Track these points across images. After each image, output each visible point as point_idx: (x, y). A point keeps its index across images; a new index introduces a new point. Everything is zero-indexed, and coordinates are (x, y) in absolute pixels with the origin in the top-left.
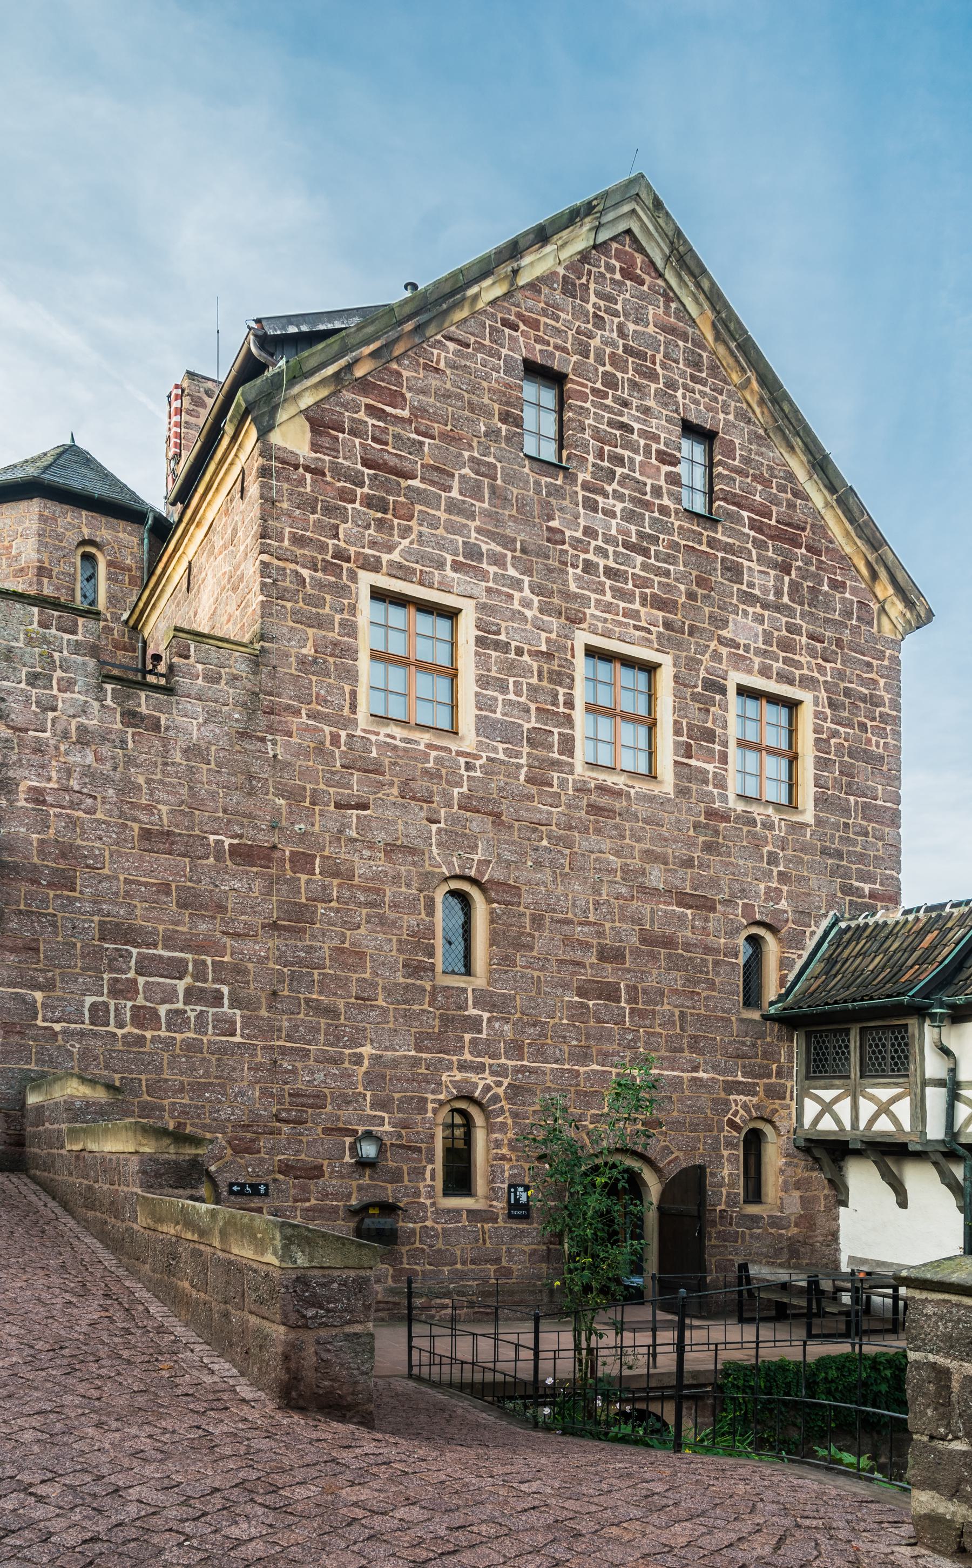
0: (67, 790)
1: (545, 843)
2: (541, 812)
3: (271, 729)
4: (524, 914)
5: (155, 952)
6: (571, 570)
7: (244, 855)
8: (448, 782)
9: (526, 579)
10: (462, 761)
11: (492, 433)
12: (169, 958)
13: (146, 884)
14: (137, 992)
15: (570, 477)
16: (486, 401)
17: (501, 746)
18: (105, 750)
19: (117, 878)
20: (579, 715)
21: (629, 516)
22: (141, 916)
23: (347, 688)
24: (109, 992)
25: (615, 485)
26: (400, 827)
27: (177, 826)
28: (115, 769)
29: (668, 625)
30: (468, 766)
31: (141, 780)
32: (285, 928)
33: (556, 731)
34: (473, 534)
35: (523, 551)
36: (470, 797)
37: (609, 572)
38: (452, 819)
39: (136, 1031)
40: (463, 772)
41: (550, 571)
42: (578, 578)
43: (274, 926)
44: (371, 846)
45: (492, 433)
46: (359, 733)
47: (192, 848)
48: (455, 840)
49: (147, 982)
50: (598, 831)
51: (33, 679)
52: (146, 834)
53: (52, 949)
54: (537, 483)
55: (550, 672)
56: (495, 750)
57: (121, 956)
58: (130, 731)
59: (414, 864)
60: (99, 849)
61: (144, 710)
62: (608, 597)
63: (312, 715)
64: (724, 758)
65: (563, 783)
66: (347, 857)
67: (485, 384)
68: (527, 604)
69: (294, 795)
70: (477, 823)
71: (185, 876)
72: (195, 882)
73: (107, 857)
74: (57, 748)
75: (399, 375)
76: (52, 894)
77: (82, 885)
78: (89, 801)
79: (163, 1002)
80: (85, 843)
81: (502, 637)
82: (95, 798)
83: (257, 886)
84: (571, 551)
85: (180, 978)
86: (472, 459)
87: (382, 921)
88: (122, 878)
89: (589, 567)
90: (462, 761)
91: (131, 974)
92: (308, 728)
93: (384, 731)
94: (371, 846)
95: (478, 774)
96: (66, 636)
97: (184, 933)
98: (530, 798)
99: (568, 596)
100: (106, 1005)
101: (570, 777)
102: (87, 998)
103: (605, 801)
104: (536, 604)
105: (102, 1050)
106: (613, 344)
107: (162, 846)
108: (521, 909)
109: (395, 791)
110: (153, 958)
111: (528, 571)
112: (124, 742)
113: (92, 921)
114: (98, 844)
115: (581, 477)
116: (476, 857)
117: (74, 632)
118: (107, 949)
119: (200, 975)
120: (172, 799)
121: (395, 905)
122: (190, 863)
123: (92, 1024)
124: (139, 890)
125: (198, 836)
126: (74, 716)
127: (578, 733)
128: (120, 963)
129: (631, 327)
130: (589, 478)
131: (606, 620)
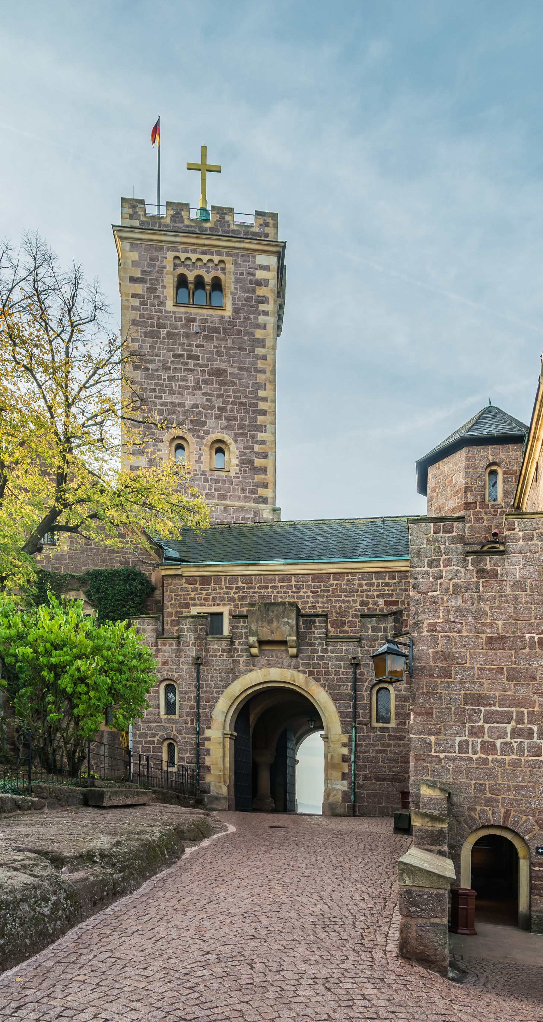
0: (447, 622)
5: (494, 708)
12: (502, 712)
13: (489, 669)
14: (484, 733)
18: (468, 595)
19: (473, 668)
22: (487, 688)
24: (469, 734)
27: (507, 632)
28: (473, 605)
31: (487, 609)
39: (483, 756)
49: (490, 727)
51: (431, 564)
52: (490, 640)
53: (439, 712)
57: (475, 713)
58: (481, 581)
60: (464, 652)
61: (489, 567)
71: (511, 661)
72: (517, 664)
73: (468, 657)
74: (442, 599)
76: (439, 681)
77: (455, 674)
78: (459, 626)
79: (499, 738)
80: (457, 650)
82: (462, 624)
85: (508, 723)
88: (476, 668)
91: (481, 723)
96: (447, 535)
97: (510, 696)
100: (467, 741)
102: (457, 738)
105: (465, 767)
107: (498, 646)
110: (493, 712)
112: (478, 588)
113: (460, 694)
114: (463, 650)
117: (451, 532)
118: (468, 710)
119: (520, 721)
122: (515, 653)
123: (460, 753)
124: (485, 673)
125: (519, 636)
126: (451, 579)
128: (475, 717)
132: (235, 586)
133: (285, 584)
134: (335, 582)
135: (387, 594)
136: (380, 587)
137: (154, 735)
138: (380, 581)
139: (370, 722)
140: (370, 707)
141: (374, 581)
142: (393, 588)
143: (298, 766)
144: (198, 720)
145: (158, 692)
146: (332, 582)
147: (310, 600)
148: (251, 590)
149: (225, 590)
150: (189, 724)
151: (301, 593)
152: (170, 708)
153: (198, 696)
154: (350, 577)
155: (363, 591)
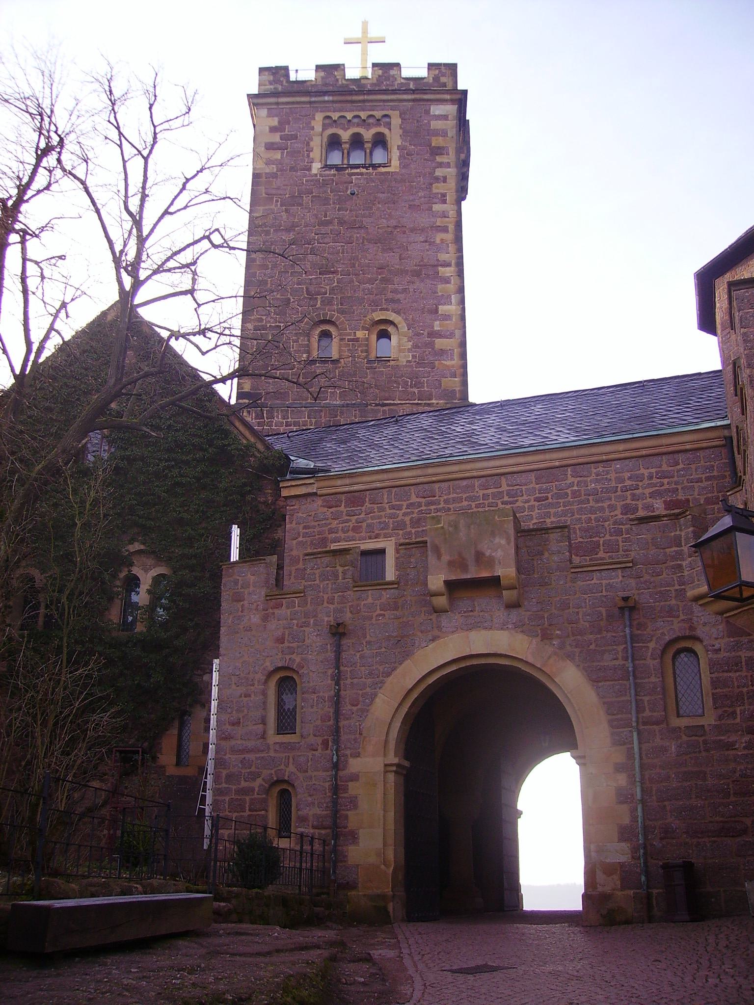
132: (405, 504)
133: (489, 491)
134: (576, 480)
135: (669, 490)
136: (655, 481)
137: (254, 776)
138: (653, 470)
139: (666, 717)
140: (664, 689)
141: (642, 471)
142: (676, 479)
143: (521, 822)
144: (337, 741)
145: (264, 694)
146: (570, 479)
147: (534, 514)
148: (432, 507)
149: (389, 511)
150: (320, 750)
151: (519, 504)
152: (286, 721)
153: (338, 695)
154: (601, 469)
155: (625, 489)
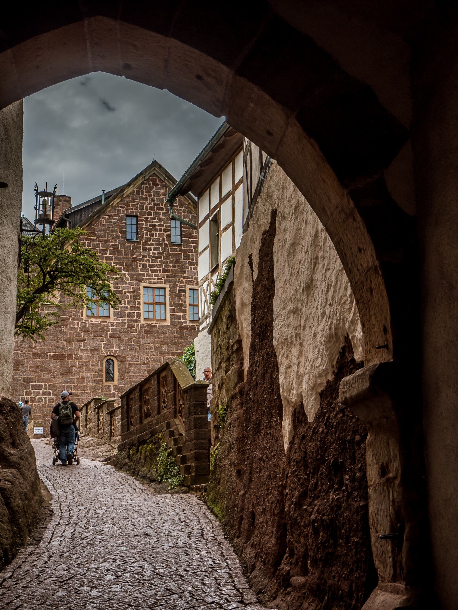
1: (132, 343)
2: (131, 335)
3: (63, 325)
4: (127, 364)
6: (139, 268)
7: (56, 357)
8: (106, 331)
9: (127, 273)
10: (110, 324)
11: (118, 237)
12: (39, 385)
13: (34, 367)
15: (139, 243)
16: (116, 229)
17: (120, 319)
20: (142, 306)
21: (155, 249)
23: (81, 311)
25: (151, 242)
26: (94, 344)
29: (167, 276)
30: (112, 326)
32: (65, 374)
33: (135, 312)
34: (113, 264)
35: (126, 266)
36: (112, 334)
37: (150, 266)
38: (107, 340)
40: (110, 327)
41: (134, 269)
42: (141, 269)
43: (63, 374)
44: (87, 350)
45: (118, 237)
46: (84, 322)
47: (44, 357)
48: (109, 345)
50: (147, 338)
54: (130, 247)
55: (134, 296)
56: (119, 320)
59: (97, 354)
62: (150, 273)
63: (72, 319)
64: (185, 311)
65: (137, 326)
66: (81, 354)
67: (116, 224)
68: (127, 279)
69: (68, 340)
70: (114, 340)
75: (94, 228)
81: (121, 290)
83: (59, 364)
84: (139, 262)
86: (112, 245)
87: (89, 370)
89: (144, 266)
90: (110, 324)
91: (30, 390)
92: (71, 323)
93: (90, 320)
94: (87, 350)
95: (114, 327)
98: (128, 331)
99: (138, 275)
101: (139, 324)
103: (149, 329)
104: (130, 279)
106: (151, 204)
108: (126, 362)
109: (93, 335)
111: (127, 270)
115: (142, 242)
116: (114, 350)
120: (40, 345)
121: (92, 365)
127: (142, 312)
129: (155, 198)
130: (144, 241)
131: (149, 279)
